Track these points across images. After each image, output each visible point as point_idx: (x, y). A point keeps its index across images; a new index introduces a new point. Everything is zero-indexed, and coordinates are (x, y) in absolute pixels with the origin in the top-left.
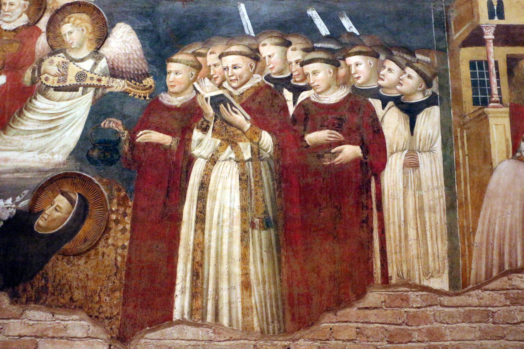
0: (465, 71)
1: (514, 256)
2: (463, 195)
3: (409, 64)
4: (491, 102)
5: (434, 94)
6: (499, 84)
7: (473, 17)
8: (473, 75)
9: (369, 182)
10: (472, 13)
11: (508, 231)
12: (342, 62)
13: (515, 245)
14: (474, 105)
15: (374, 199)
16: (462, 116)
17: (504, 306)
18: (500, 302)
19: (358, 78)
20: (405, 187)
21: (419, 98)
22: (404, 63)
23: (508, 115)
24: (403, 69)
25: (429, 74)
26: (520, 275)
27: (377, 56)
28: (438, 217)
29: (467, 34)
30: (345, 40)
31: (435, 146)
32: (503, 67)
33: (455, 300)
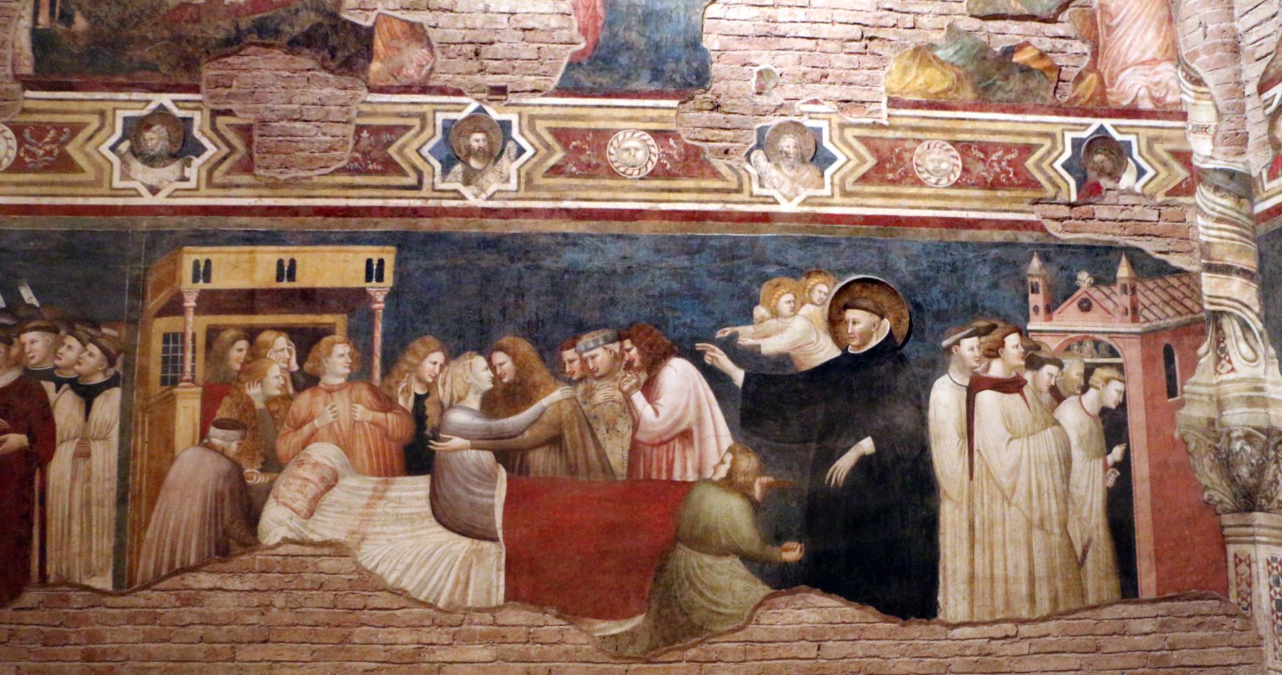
0: (157, 345)
1: (187, 554)
2: (137, 488)
3: (93, 340)
4: (182, 381)
5: (117, 374)
6: (194, 359)
7: (174, 280)
8: (165, 350)
9: (33, 474)
10: (173, 276)
11: (183, 526)
12: (15, 340)
13: (190, 541)
14: (162, 385)
15: (37, 492)
16: (146, 399)
17: (174, 607)
18: (170, 603)
19: (33, 357)
20: (73, 479)
21: (99, 379)
22: (86, 338)
23: (199, 396)
24: (84, 345)
25: (113, 351)
26: (194, 574)
27: (56, 331)
28: (106, 510)
29: (164, 302)
30: (22, 313)
31: (112, 432)
32: (201, 340)
33: (120, 601)
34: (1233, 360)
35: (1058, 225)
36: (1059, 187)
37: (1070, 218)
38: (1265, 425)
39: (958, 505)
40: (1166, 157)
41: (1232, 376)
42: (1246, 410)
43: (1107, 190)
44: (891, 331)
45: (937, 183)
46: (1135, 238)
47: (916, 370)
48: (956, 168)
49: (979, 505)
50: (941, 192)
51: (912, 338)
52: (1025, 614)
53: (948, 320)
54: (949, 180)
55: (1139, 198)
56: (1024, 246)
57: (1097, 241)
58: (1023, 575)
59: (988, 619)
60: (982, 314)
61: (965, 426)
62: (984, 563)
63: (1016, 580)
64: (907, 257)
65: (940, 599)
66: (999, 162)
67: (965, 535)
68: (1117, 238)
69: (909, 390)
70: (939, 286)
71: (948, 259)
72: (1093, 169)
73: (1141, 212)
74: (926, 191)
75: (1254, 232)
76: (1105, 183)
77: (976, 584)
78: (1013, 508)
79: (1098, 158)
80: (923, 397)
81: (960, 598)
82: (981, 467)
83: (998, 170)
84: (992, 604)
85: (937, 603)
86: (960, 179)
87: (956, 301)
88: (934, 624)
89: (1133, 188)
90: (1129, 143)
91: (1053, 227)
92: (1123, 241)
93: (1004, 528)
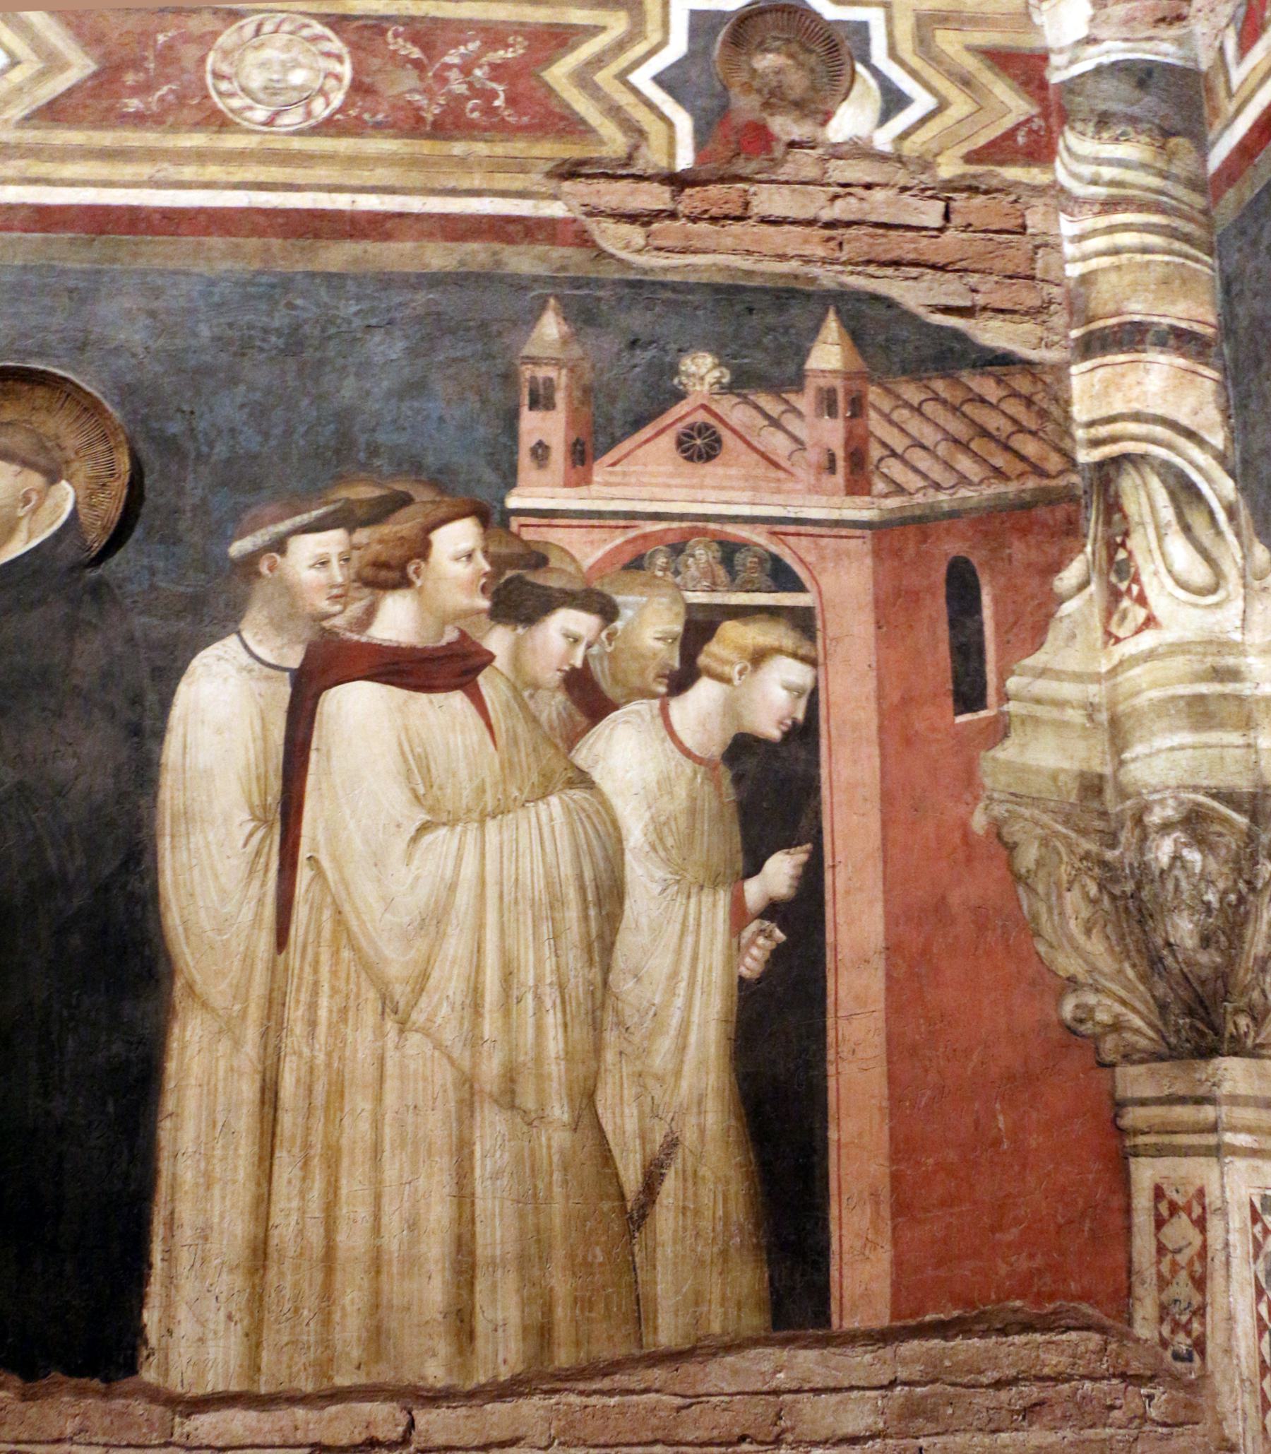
34: (1151, 594)
35: (636, 234)
36: (641, 133)
37: (673, 215)
38: (1243, 784)
39: (229, 1028)
40: (971, 64)
41: (1148, 640)
42: (1186, 738)
43: (792, 145)
44: (74, 513)
45: (270, 122)
46: (872, 269)
47: (139, 622)
48: (332, 82)
49: (299, 1029)
50: (278, 144)
51: (138, 532)
52: (435, 1373)
53: (256, 486)
54: (309, 114)
55: (888, 168)
56: (519, 285)
57: (749, 274)
58: (435, 1249)
59: (307, 1385)
60: (363, 466)
61: (276, 785)
62: (303, 1211)
63: (412, 1262)
64: (152, 314)
65: (151, 1317)
66: (466, 69)
67: (245, 1121)
68: (815, 270)
69: (106, 676)
70: (242, 388)
71: (280, 320)
72: (747, 88)
73: (888, 203)
74: (232, 142)
75: (1210, 227)
76: (785, 126)
77: (272, 1274)
78: (414, 1038)
79: (767, 62)
80: (151, 698)
81: (217, 1319)
82: (316, 909)
83: (461, 89)
84: (326, 1343)
85: (139, 1332)
86: (340, 110)
87: (288, 432)
88: (126, 1395)
89: (870, 139)
90: (861, 29)
91: (614, 236)
92: (827, 277)
93: (379, 1099)
